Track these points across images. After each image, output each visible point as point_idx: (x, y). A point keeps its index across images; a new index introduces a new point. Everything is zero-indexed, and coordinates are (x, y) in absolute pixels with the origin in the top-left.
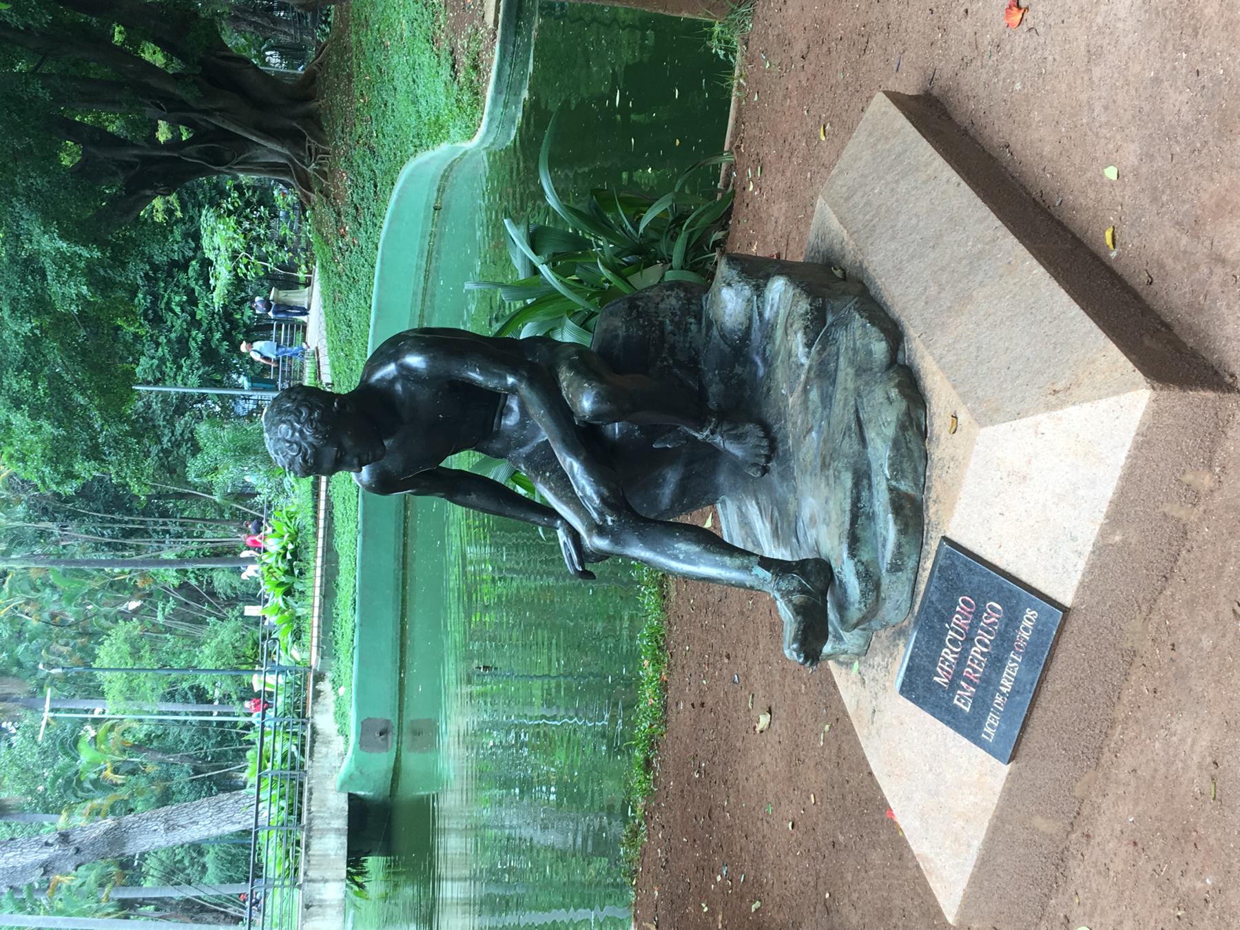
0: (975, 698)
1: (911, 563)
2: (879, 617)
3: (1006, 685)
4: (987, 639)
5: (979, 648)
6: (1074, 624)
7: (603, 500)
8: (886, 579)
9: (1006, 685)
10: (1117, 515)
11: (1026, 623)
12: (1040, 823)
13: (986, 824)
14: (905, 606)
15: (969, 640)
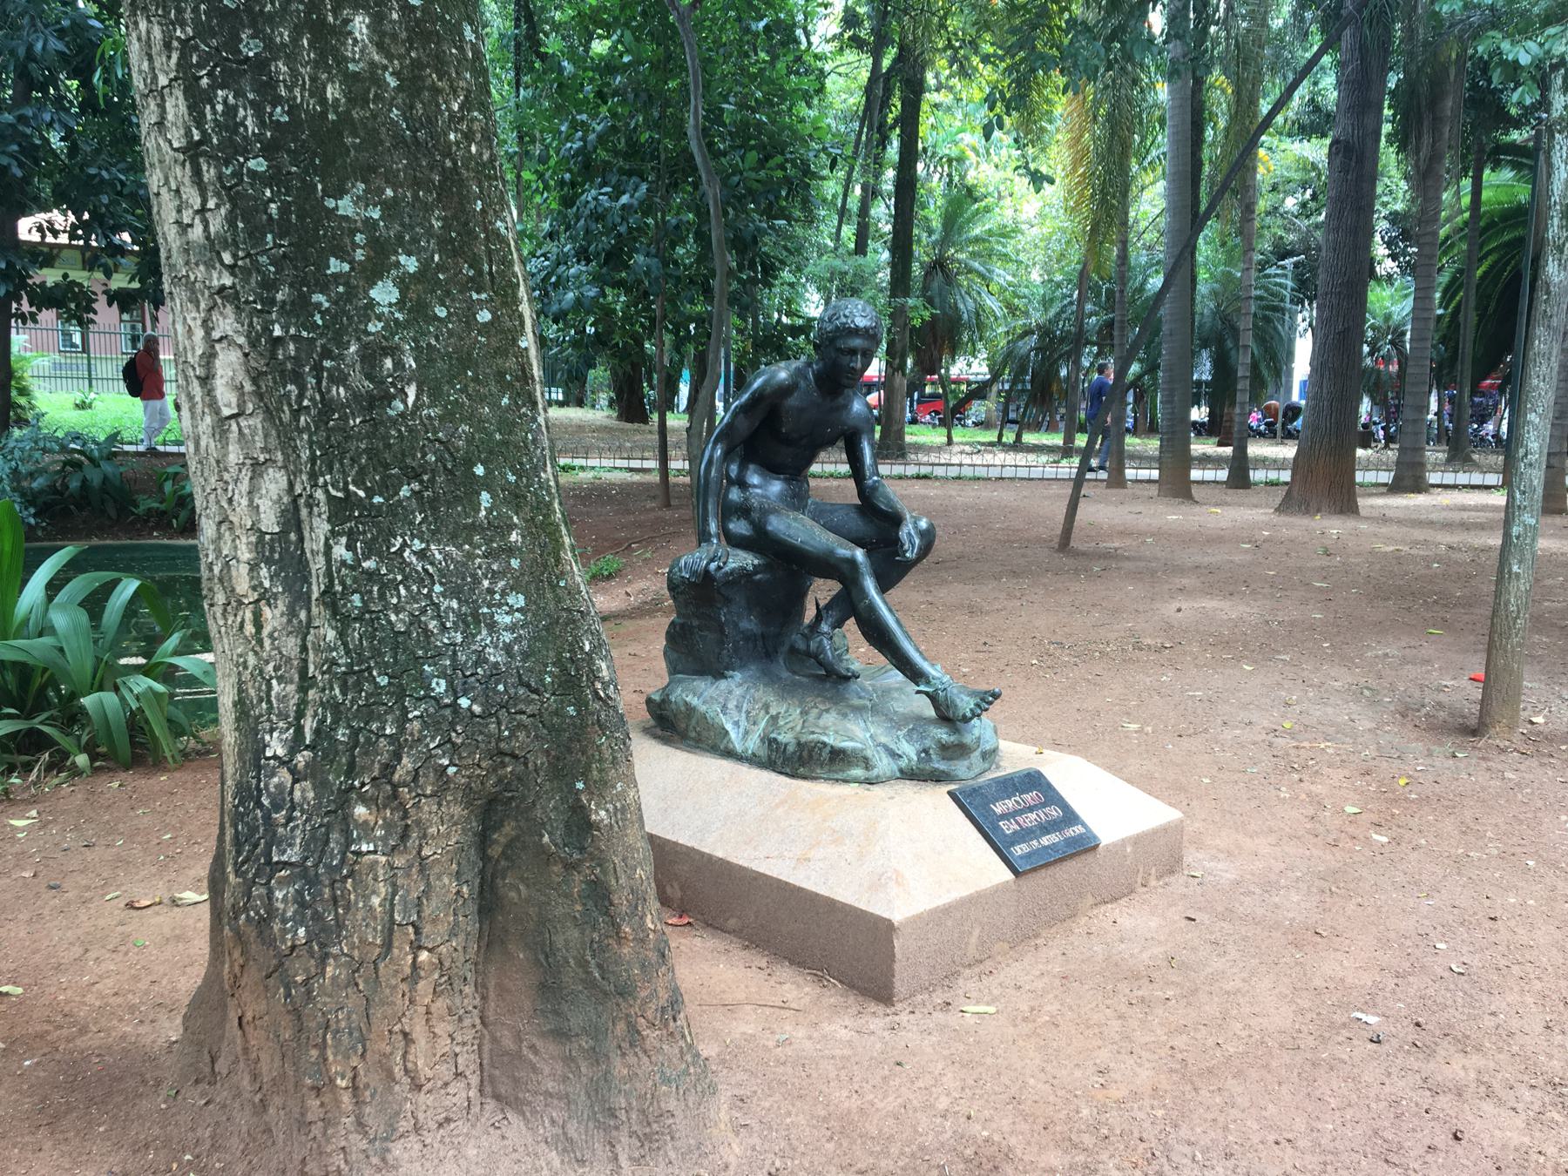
0: (1015, 832)
1: (987, 765)
2: (951, 762)
3: (1046, 841)
4: (1042, 816)
5: (1034, 816)
6: (1089, 858)
7: (920, 548)
8: (977, 753)
9: (1046, 841)
10: (1137, 840)
11: (1075, 828)
12: (976, 932)
13: (972, 891)
14: (972, 774)
15: (1031, 809)
